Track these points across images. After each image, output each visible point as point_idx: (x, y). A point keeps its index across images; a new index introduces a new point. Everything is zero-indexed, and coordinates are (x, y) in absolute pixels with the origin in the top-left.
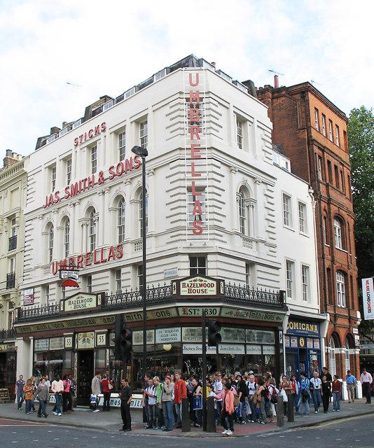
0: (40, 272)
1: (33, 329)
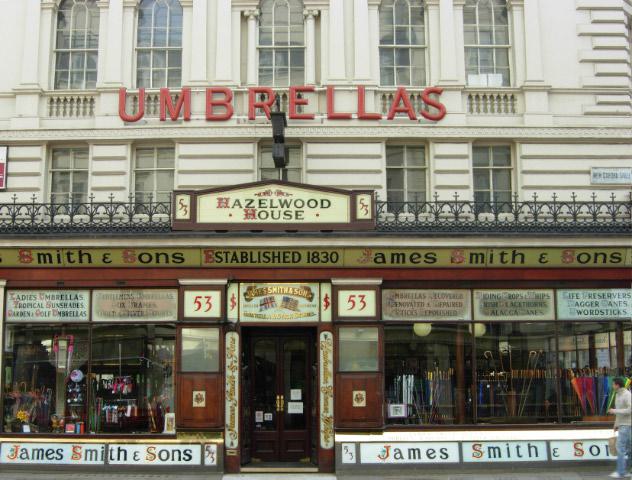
0: (30, 105)
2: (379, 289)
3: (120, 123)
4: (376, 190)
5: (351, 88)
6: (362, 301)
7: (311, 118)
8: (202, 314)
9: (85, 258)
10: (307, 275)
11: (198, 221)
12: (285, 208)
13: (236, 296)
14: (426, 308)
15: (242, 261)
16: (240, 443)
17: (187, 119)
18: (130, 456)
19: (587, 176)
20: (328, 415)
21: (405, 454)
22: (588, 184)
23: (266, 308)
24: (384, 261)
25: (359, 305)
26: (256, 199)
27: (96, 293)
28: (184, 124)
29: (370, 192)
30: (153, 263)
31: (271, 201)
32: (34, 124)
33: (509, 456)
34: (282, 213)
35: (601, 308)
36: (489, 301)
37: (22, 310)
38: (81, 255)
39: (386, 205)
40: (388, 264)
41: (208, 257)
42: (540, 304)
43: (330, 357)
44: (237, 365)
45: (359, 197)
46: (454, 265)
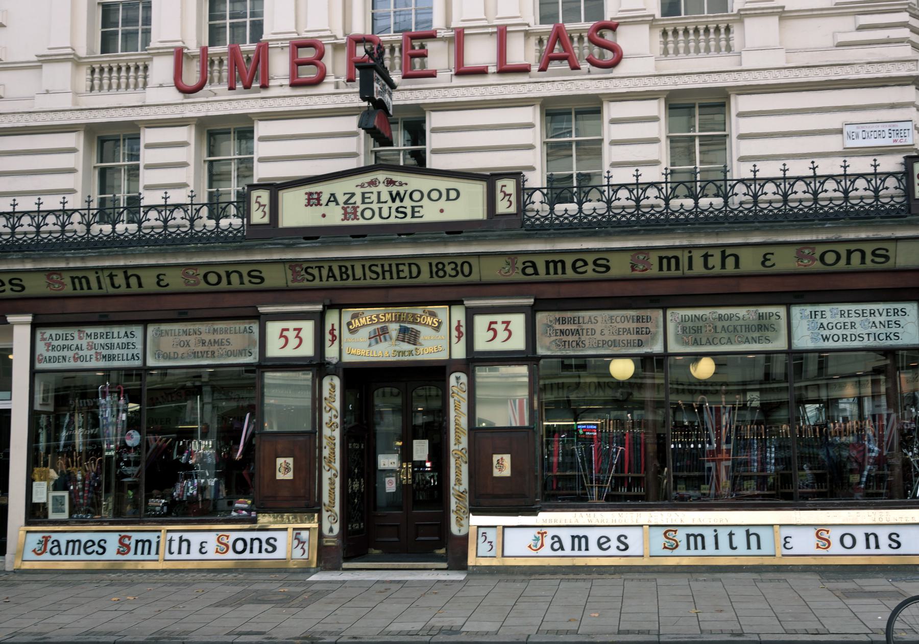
1: (36, 286)
2: (531, 314)
3: (177, 97)
4: (527, 174)
5: (490, 30)
6: (506, 329)
7: (432, 75)
8: (290, 352)
9: (133, 281)
10: (429, 294)
11: (280, 226)
12: (398, 203)
13: (337, 327)
14: (598, 336)
15: (342, 279)
16: (343, 527)
17: (265, 86)
18: (195, 548)
19: (838, 137)
20: (462, 489)
21: (567, 543)
22: (840, 149)
23: (377, 343)
24: (536, 273)
25: (501, 334)
26: (358, 192)
27: (151, 329)
28: (264, 93)
29: (516, 175)
30: (224, 285)
31: (379, 193)
32: (66, 102)
33: (717, 548)
34: (393, 210)
35: (859, 330)
36: (690, 324)
37: (56, 354)
38: (127, 278)
39: (205, 209)
40: (542, 275)
41: (295, 273)
42: (764, 327)
43: (464, 407)
44: (338, 420)
45: (499, 183)
46: (637, 274)
